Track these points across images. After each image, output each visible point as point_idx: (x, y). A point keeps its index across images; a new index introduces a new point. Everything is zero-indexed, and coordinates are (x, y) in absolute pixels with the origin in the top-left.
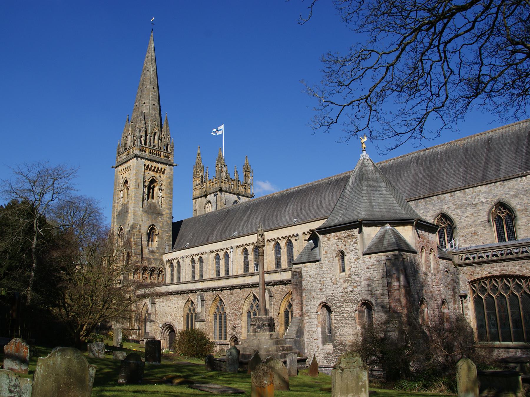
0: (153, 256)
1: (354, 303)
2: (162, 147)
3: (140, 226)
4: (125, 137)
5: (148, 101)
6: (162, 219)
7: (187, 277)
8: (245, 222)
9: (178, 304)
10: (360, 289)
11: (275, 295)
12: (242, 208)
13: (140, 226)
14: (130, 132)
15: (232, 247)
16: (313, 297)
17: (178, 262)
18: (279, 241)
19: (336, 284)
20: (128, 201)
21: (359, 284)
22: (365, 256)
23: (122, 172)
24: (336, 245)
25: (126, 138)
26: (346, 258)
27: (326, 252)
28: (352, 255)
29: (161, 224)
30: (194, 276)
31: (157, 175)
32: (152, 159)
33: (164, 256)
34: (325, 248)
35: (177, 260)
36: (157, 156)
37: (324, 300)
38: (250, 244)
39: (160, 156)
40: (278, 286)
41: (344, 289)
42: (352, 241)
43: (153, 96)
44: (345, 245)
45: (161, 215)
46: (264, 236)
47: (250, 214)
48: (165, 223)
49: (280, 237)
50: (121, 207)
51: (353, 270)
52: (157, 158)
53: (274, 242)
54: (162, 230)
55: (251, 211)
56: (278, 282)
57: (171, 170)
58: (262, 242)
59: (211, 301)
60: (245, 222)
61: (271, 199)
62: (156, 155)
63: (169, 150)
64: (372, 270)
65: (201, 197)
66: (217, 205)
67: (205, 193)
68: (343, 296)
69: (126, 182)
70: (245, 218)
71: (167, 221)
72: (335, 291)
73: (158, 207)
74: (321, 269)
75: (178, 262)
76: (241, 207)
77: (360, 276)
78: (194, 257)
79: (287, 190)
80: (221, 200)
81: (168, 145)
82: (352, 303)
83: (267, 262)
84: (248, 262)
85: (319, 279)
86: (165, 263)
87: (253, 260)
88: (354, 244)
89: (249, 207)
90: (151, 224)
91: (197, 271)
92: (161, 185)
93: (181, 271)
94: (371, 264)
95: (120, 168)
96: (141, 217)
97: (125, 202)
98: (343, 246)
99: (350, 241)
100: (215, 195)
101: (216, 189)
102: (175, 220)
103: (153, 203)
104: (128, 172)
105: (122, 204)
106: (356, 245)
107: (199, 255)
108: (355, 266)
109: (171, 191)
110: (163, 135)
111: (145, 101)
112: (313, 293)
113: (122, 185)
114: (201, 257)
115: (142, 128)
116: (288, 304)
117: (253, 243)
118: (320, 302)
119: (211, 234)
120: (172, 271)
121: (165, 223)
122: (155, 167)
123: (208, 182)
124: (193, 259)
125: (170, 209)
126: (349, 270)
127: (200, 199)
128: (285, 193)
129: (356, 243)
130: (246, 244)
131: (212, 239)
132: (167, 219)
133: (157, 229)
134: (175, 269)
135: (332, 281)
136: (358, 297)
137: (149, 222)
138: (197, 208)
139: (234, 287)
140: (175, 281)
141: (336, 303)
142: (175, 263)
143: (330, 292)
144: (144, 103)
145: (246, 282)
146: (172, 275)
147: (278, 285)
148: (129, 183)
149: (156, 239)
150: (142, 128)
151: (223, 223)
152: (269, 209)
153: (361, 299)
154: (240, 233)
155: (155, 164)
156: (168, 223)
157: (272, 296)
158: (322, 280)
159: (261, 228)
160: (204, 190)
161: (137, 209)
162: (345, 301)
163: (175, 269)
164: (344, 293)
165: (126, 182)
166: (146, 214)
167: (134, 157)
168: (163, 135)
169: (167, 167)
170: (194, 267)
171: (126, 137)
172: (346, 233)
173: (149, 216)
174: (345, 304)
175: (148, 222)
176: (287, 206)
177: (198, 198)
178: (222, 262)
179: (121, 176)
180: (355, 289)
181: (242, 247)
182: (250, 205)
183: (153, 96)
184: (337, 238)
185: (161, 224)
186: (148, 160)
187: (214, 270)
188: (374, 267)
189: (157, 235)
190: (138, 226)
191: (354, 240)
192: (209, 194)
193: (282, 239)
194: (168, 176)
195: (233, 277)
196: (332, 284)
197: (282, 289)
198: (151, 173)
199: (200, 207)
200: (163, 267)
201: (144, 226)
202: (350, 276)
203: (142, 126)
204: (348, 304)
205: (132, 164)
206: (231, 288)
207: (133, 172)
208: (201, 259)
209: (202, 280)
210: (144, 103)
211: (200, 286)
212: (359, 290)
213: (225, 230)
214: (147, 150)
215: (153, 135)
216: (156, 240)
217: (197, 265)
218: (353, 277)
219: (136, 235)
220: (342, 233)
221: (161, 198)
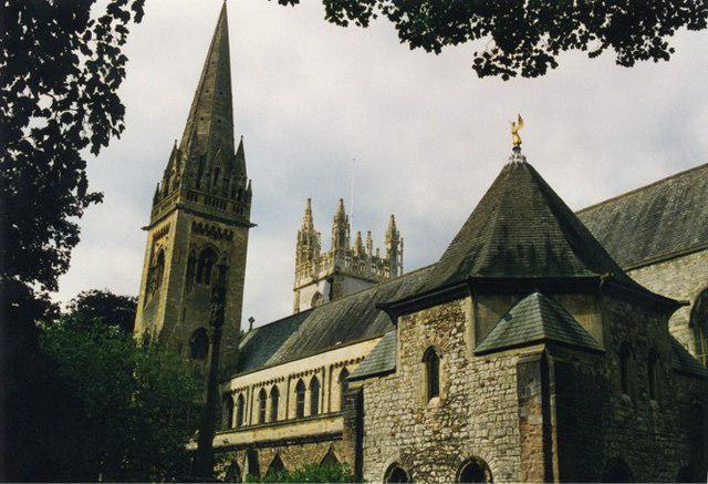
1: (453, 466)
10: (466, 434)
14: (174, 168)
16: (379, 451)
17: (241, 397)
22: (477, 359)
24: (424, 336)
26: (442, 363)
28: (454, 356)
31: (217, 243)
34: (405, 345)
41: (435, 433)
44: (442, 336)
51: (453, 389)
64: (491, 389)
68: (431, 450)
72: (418, 439)
75: (241, 397)
85: (391, 413)
88: (458, 332)
91: (268, 413)
92: (224, 259)
94: (487, 375)
106: (460, 335)
108: (457, 381)
112: (378, 443)
122: (213, 228)
126: (447, 389)
129: (460, 330)
130: (346, 362)
141: (418, 465)
142: (236, 398)
153: (466, 455)
155: (211, 224)
158: (397, 413)
164: (434, 444)
165: (162, 255)
170: (263, 405)
174: (435, 467)
178: (308, 395)
180: (456, 435)
184: (427, 321)
186: (201, 215)
191: (458, 324)
202: (445, 404)
206: (300, 441)
207: (172, 234)
208: (275, 392)
209: (275, 424)
211: (248, 437)
212: (462, 435)
217: (269, 401)
218: (453, 406)
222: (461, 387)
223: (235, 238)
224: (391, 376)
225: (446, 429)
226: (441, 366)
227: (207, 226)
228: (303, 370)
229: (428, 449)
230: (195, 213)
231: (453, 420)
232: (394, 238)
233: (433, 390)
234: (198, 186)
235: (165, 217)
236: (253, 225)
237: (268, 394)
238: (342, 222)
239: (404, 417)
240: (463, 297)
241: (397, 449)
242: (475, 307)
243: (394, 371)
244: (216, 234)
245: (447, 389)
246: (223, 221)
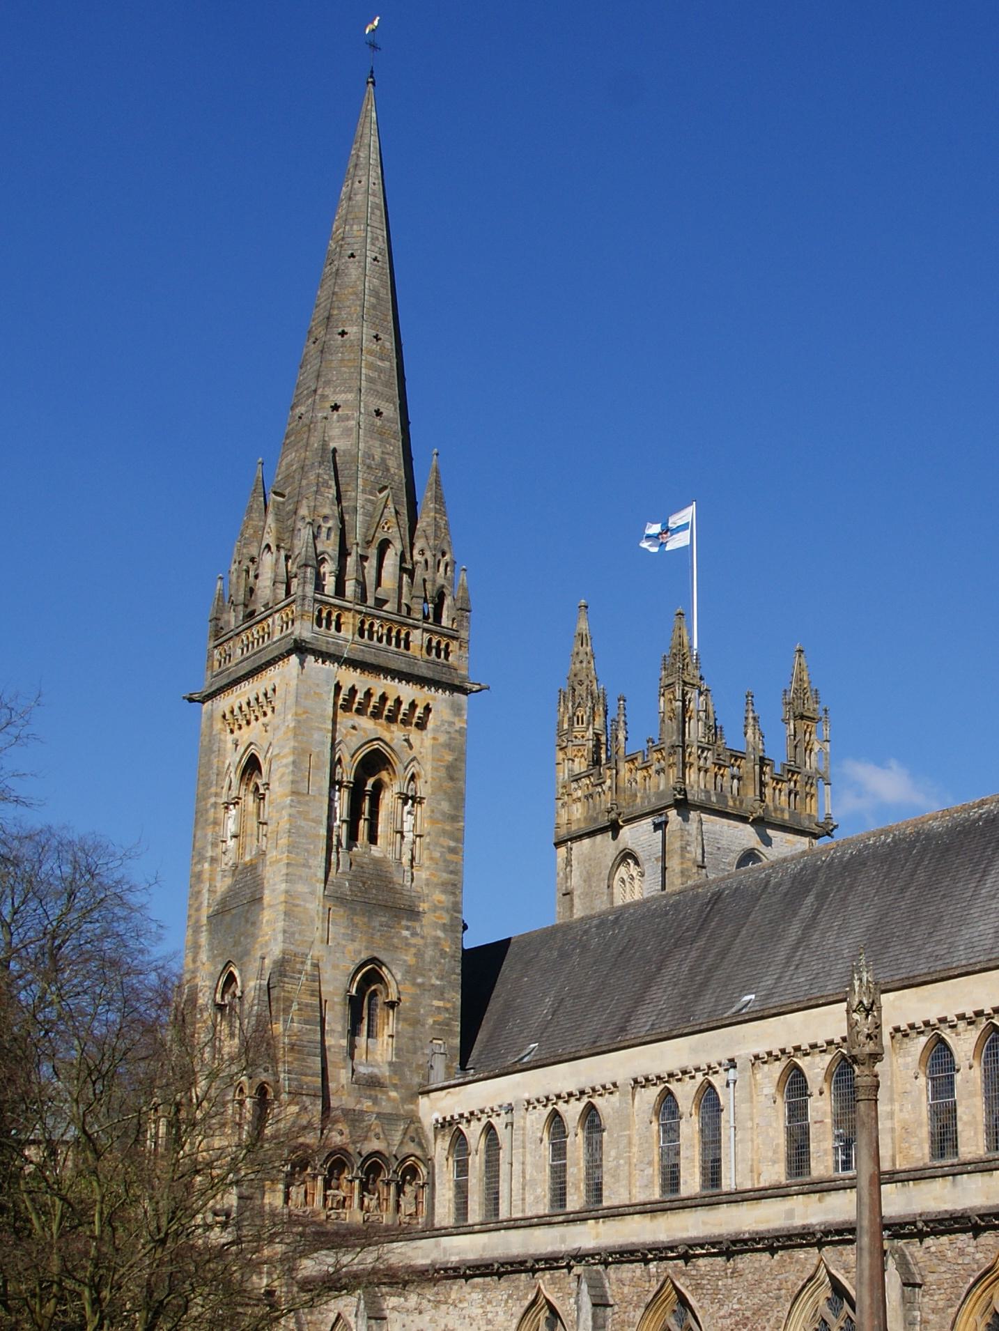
0: (375, 1101)
2: (417, 606)
3: (316, 966)
4: (247, 563)
5: (350, 396)
6: (414, 934)
7: (530, 1198)
8: (795, 949)
9: (489, 1322)
11: (930, 1278)
12: (779, 884)
13: (316, 966)
14: (270, 539)
15: (732, 1063)
17: (489, 1128)
18: (947, 1034)
20: (262, 854)
23: (234, 720)
25: (252, 567)
29: (410, 959)
30: (559, 1195)
31: (395, 735)
32: (370, 659)
33: (423, 1101)
35: (484, 1121)
36: (393, 647)
38: (813, 1046)
39: (407, 647)
40: (944, 1239)
43: (375, 375)
45: (413, 914)
46: (879, 1009)
47: (817, 912)
48: (429, 953)
49: (951, 1017)
50: (228, 881)
52: (390, 655)
53: (923, 1040)
54: (414, 984)
55: (822, 897)
56: (940, 1221)
57: (457, 710)
58: (869, 1036)
59: (637, 1306)
60: (795, 949)
61: (912, 845)
62: (389, 642)
63: (445, 622)
65: (591, 834)
66: (664, 869)
67: (613, 816)
69: (252, 766)
70: (794, 930)
71: (437, 942)
73: (397, 879)
76: (773, 881)
78: (561, 1107)
79: (983, 803)
80: (683, 849)
81: (441, 596)
83: (893, 1130)
84: (805, 1132)
86: (431, 1135)
87: (829, 1120)
89: (813, 881)
90: (364, 956)
92: (413, 777)
93: (504, 1169)
95: (224, 703)
96: (318, 924)
97: (247, 858)
100: (657, 827)
101: (660, 795)
102: (472, 940)
103: (376, 862)
104: (262, 719)
105: (236, 866)
107: (585, 1099)
109: (456, 808)
110: (422, 552)
111: (339, 399)
113: (235, 777)
114: (591, 1109)
115: (326, 518)
116: (989, 1319)
117: (830, 1043)
119: (639, 1001)
120: (462, 1168)
121: (429, 953)
122: (384, 698)
123: (624, 767)
124: (555, 1117)
125: (453, 888)
127: (586, 842)
128: (974, 813)
130: (797, 1049)
131: (641, 1024)
132: (440, 934)
133: (394, 977)
134: (476, 1162)
137: (356, 945)
138: (575, 881)
139: (745, 1242)
140: (475, 1214)
142: (473, 1132)
144: (336, 408)
145: (798, 1222)
146: (461, 1190)
147: (942, 1233)
148: (264, 768)
149: (388, 1026)
150: (326, 518)
151: (694, 954)
152: (902, 890)
154: (769, 996)
156: (443, 954)
157: (915, 1285)
159: (865, 976)
160: (606, 800)
161: (301, 888)
163: (476, 1162)
165: (252, 766)
166: (341, 911)
167: (289, 653)
168: (422, 552)
169: (439, 700)
170: (559, 1150)
171: (252, 560)
173: (357, 919)
175: (352, 947)
176: (985, 873)
177: (579, 837)
178: (690, 1128)
179: (230, 738)
181: (777, 1059)
182: (817, 870)
183: (375, 375)
185: (410, 959)
186: (353, 663)
187: (650, 1163)
189: (392, 1005)
190: (308, 967)
192: (629, 821)
193: (962, 1025)
194: (443, 738)
195: (740, 1197)
197: (962, 1253)
198: (365, 723)
199: (588, 879)
200: (419, 1153)
201: (335, 967)
203: (326, 511)
205: (277, 681)
206: (731, 1247)
207: (284, 719)
210: (336, 408)
211: (589, 1236)
213: (704, 984)
214: (347, 618)
215: (373, 552)
216: (388, 1030)
217: (576, 1142)
219: (295, 1007)
221: (409, 837)
228: (674, 1067)
234: (340, 591)
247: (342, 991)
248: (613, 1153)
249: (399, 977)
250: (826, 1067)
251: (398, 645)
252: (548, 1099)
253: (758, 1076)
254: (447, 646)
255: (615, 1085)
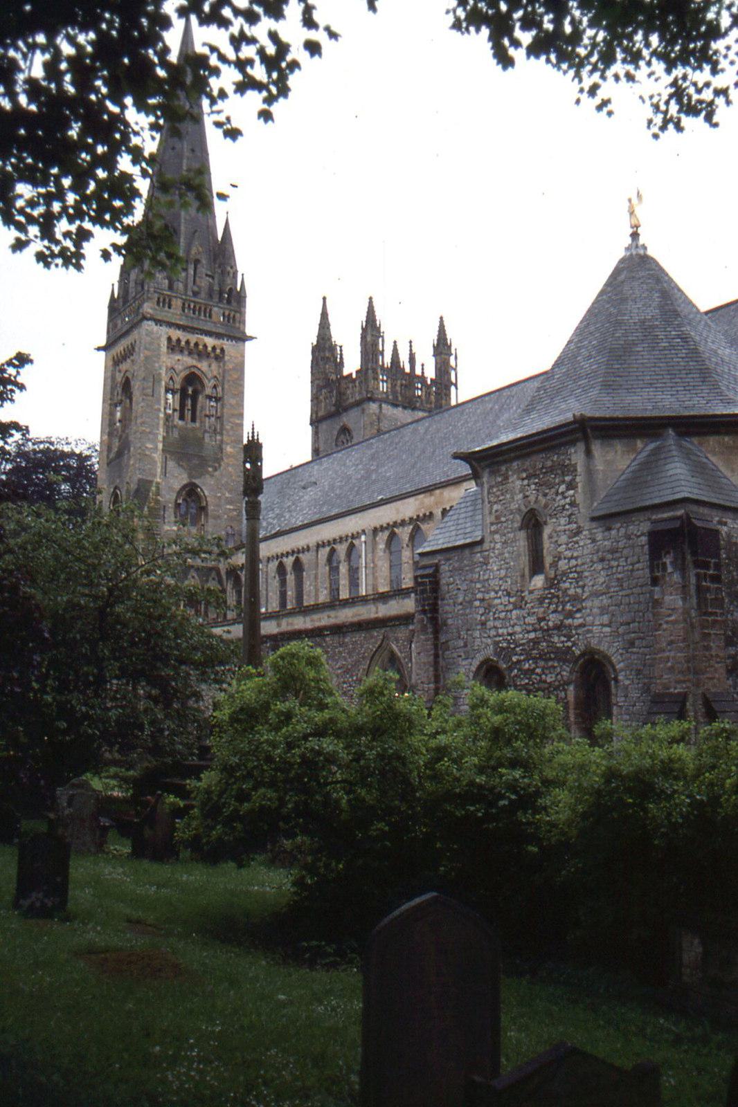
1: (565, 661)
10: (581, 621)
13: (158, 488)
19: (521, 607)
21: (579, 606)
24: (521, 496)
26: (547, 531)
27: (497, 518)
28: (563, 521)
31: (203, 365)
34: (495, 507)
37: (489, 652)
41: (540, 620)
42: (563, 481)
44: (545, 495)
51: (563, 565)
64: (614, 563)
68: (536, 642)
72: (518, 629)
74: (484, 567)
77: (581, 583)
78: (285, 559)
82: (559, 660)
85: (479, 596)
86: (224, 577)
88: (568, 489)
92: (215, 387)
98: (540, 497)
99: (557, 481)
104: (132, 358)
106: (571, 492)
107: (295, 555)
108: (568, 554)
118: (479, 658)
122: (196, 344)
126: (554, 564)
129: (571, 486)
135: (512, 600)
136: (574, 644)
141: (519, 662)
143: (505, 631)
153: (583, 648)
155: (193, 338)
162: (542, 656)
164: (539, 634)
169: (227, 344)
170: (283, 583)
172: (547, 458)
174: (542, 663)
181: (386, 528)
184: (524, 475)
186: (178, 327)
187: (326, 588)
188: (618, 555)
191: (567, 478)
196: (511, 607)
202: (552, 583)
204: (550, 663)
208: (298, 566)
212: (577, 622)
217: (290, 578)
220: (538, 461)
222: (573, 562)
223: (227, 358)
224: (478, 549)
225: (554, 615)
226: (545, 536)
227: (188, 342)
229: (531, 640)
230: (170, 325)
231: (564, 604)
232: (442, 348)
233: (537, 565)
235: (127, 333)
236: (251, 338)
237: (289, 568)
238: (371, 331)
239: (497, 601)
240: (573, 443)
241: (489, 641)
242: (588, 453)
243: (481, 542)
244: (200, 352)
245: (554, 564)
246: (209, 333)
247: (173, 501)
248: (308, 583)
249: (206, 493)
250: (410, 531)
251: (205, 316)
252: (277, 556)
253: (377, 539)
254: (234, 317)
255: (308, 547)
